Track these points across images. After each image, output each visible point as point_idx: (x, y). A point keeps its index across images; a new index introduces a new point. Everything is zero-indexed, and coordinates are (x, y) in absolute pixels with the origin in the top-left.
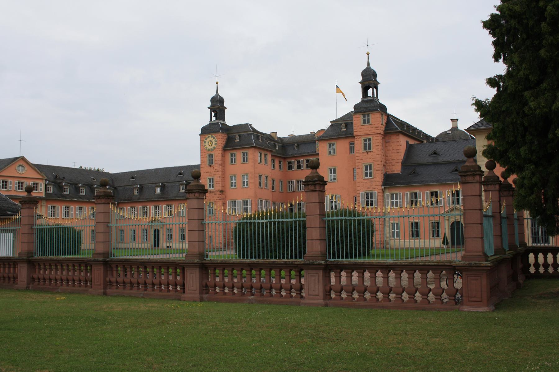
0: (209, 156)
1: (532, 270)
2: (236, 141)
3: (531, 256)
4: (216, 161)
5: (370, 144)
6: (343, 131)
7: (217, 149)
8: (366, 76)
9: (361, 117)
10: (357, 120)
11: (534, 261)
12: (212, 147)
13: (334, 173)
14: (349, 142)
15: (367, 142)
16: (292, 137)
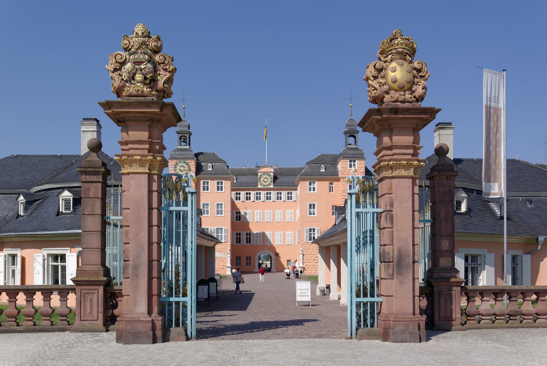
8: (351, 126)
9: (349, 161)
10: (345, 164)
13: (314, 208)
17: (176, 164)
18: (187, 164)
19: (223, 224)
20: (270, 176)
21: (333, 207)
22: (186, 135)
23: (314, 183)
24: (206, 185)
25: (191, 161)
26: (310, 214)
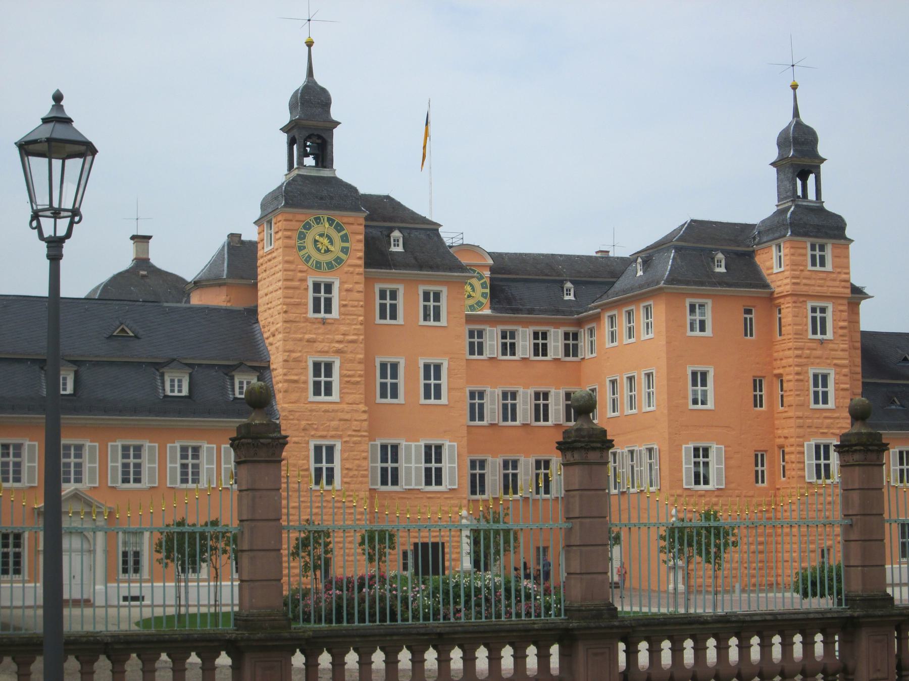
0: (317, 287)
4: (345, 306)
5: (823, 320)
6: (720, 273)
7: (351, 269)
12: (329, 258)
13: (704, 383)
14: (744, 306)
15: (818, 315)
17: (304, 227)
18: (339, 228)
19: (445, 432)
20: (480, 278)
21: (755, 381)
22: (324, 135)
23: (702, 306)
24: (388, 302)
25: (351, 220)
26: (695, 402)
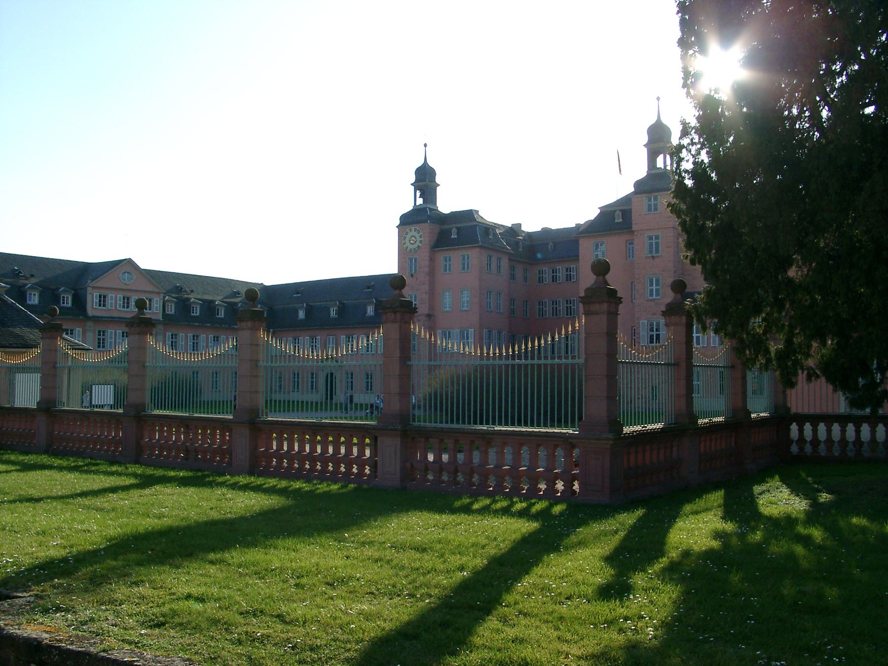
1: (794, 449)
2: (452, 237)
3: (794, 427)
5: (657, 244)
6: (618, 223)
11: (854, 438)
12: (416, 246)
16: (546, 232)
